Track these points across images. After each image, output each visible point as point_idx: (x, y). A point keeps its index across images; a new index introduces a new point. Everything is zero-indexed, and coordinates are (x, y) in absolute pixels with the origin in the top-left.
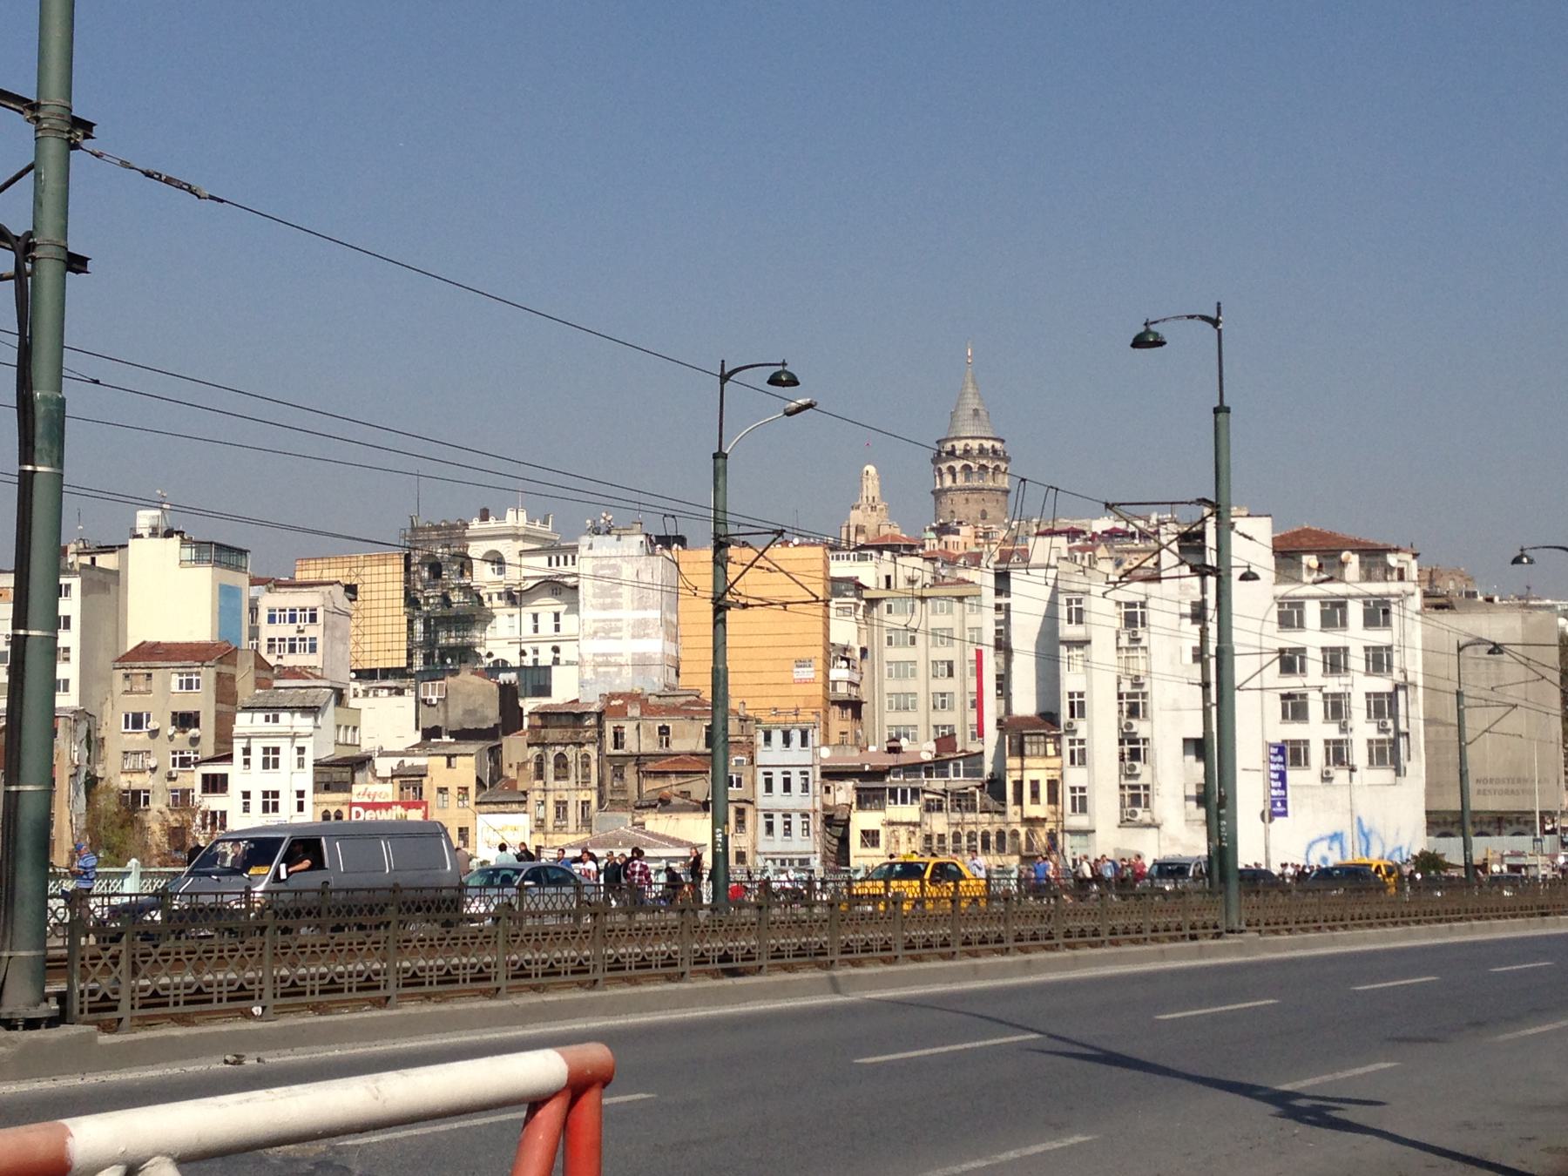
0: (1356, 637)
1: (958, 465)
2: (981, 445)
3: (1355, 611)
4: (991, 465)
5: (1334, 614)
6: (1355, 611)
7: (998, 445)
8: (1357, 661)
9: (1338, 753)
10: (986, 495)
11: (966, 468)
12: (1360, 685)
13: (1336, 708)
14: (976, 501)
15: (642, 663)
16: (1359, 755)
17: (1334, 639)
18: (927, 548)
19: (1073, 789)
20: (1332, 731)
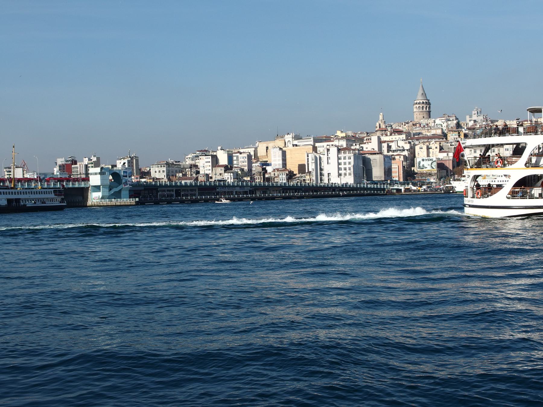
0: (347, 161)
2: (423, 102)
3: (347, 158)
4: (425, 106)
5: (345, 158)
6: (347, 158)
7: (427, 101)
8: (347, 163)
9: (345, 174)
10: (424, 113)
12: (347, 166)
14: (422, 114)
15: (279, 164)
16: (348, 174)
17: (345, 161)
18: (389, 130)
20: (345, 172)
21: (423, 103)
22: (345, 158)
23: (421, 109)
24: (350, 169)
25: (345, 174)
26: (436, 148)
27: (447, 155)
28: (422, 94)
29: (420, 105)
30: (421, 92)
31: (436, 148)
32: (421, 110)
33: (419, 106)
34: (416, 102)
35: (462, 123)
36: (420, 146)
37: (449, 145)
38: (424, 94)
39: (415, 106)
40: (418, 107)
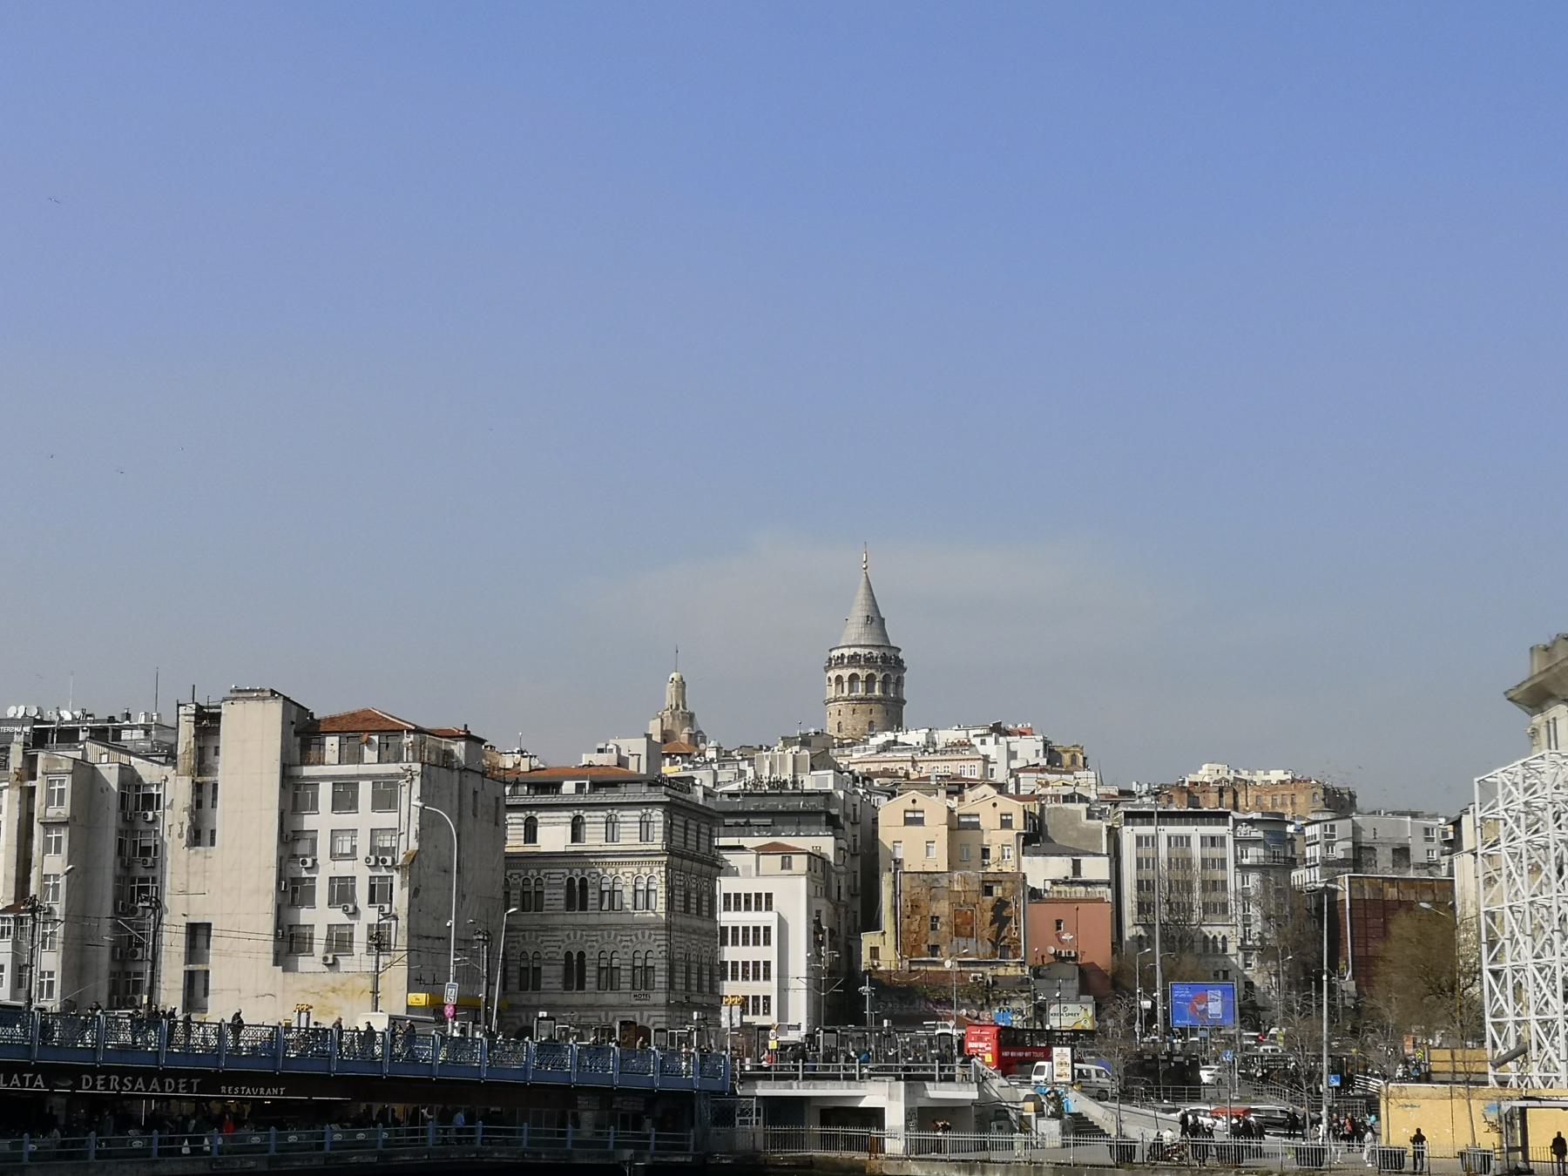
0: (365, 818)
1: (846, 673)
3: (365, 790)
4: (879, 676)
5: (345, 798)
6: (365, 790)
10: (876, 707)
11: (853, 678)
13: (342, 892)
17: (345, 820)
19: (42, 974)
20: (338, 916)
21: (869, 660)
22: (345, 798)
24: (379, 893)
25: (340, 942)
26: (1006, 824)
27: (1076, 867)
29: (857, 671)
31: (1006, 824)
32: (860, 690)
33: (853, 671)
34: (836, 653)
36: (911, 806)
37: (1080, 812)
38: (875, 620)
39: (833, 674)
40: (846, 679)
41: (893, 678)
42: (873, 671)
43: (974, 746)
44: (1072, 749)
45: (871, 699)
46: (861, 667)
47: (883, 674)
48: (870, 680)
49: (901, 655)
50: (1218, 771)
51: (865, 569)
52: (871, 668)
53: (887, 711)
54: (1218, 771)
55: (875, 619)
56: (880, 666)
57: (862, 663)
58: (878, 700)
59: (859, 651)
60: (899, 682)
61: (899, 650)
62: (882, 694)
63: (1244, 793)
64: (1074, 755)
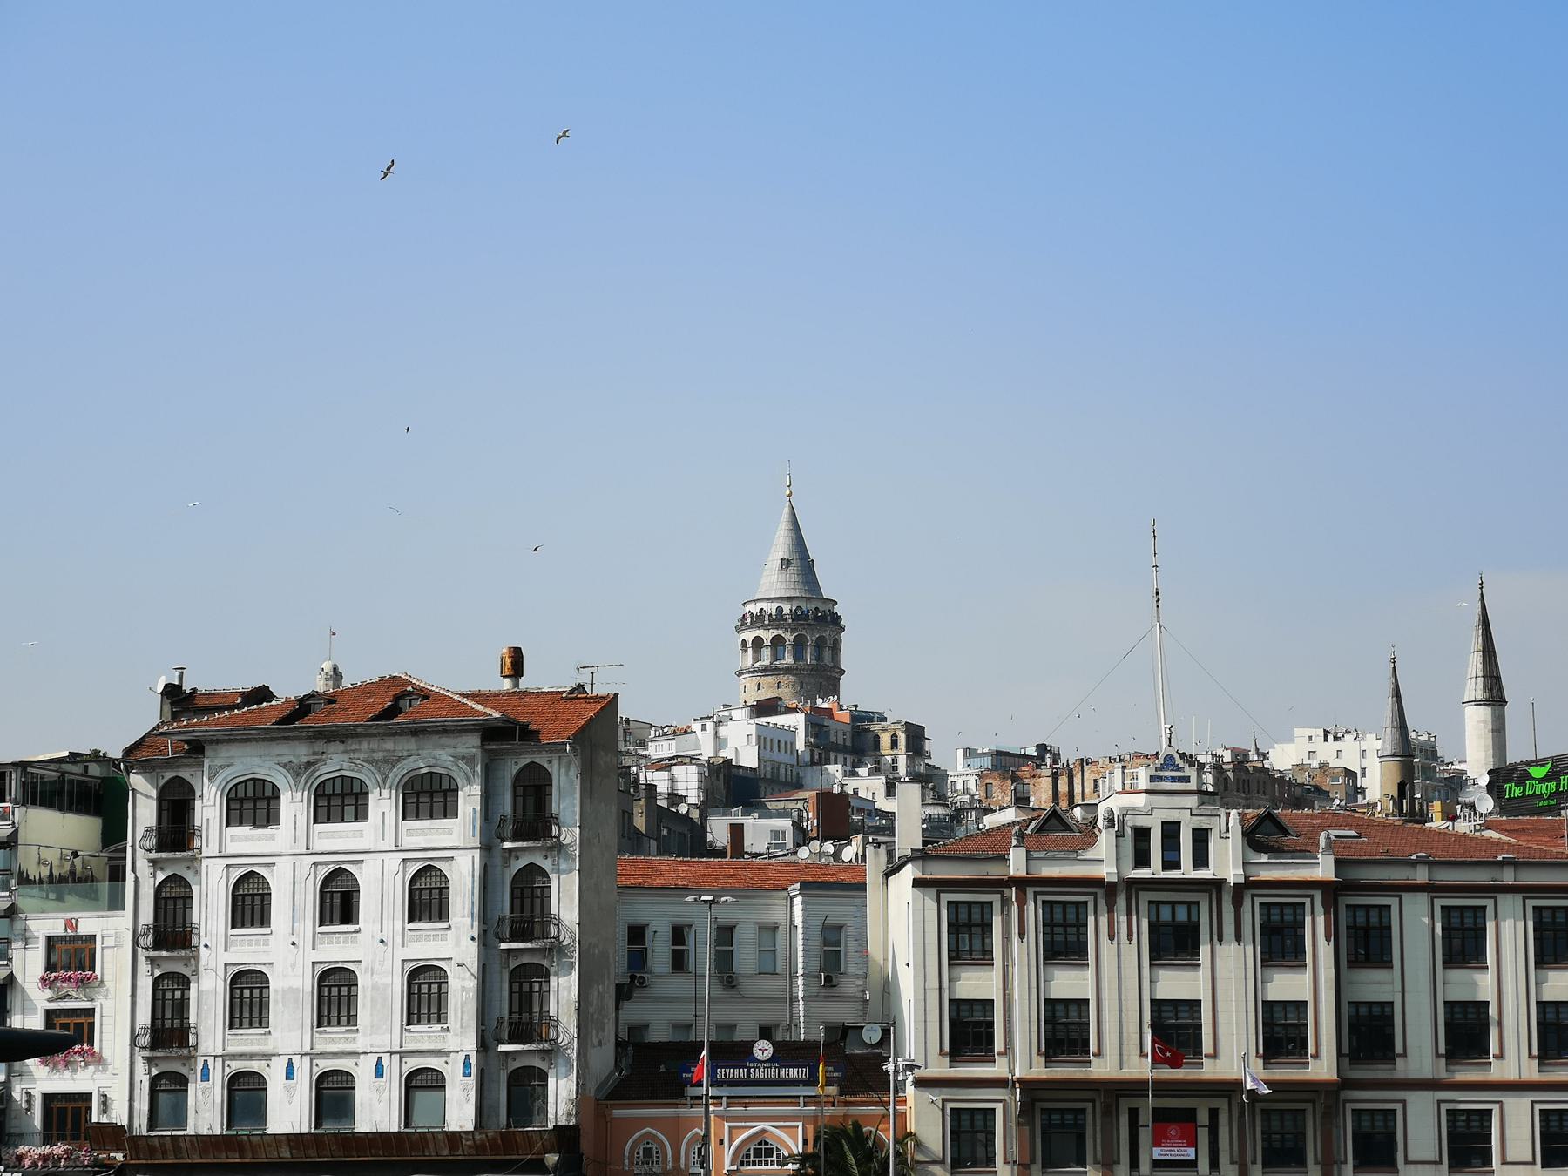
2: (780, 610)
4: (789, 637)
10: (786, 679)
23: (766, 653)
28: (785, 563)
30: (780, 547)
35: (884, 730)
38: (801, 562)
41: (811, 638)
42: (780, 632)
43: (695, 732)
44: (892, 727)
45: (777, 669)
46: (766, 628)
47: (793, 637)
48: (777, 642)
49: (836, 609)
50: (1310, 738)
51: (789, 496)
52: (777, 629)
53: (802, 683)
54: (1310, 738)
55: (794, 562)
56: (789, 624)
57: (766, 622)
58: (788, 670)
59: (764, 605)
60: (836, 647)
61: (836, 603)
62: (814, 662)
63: (1079, 775)
64: (895, 735)
